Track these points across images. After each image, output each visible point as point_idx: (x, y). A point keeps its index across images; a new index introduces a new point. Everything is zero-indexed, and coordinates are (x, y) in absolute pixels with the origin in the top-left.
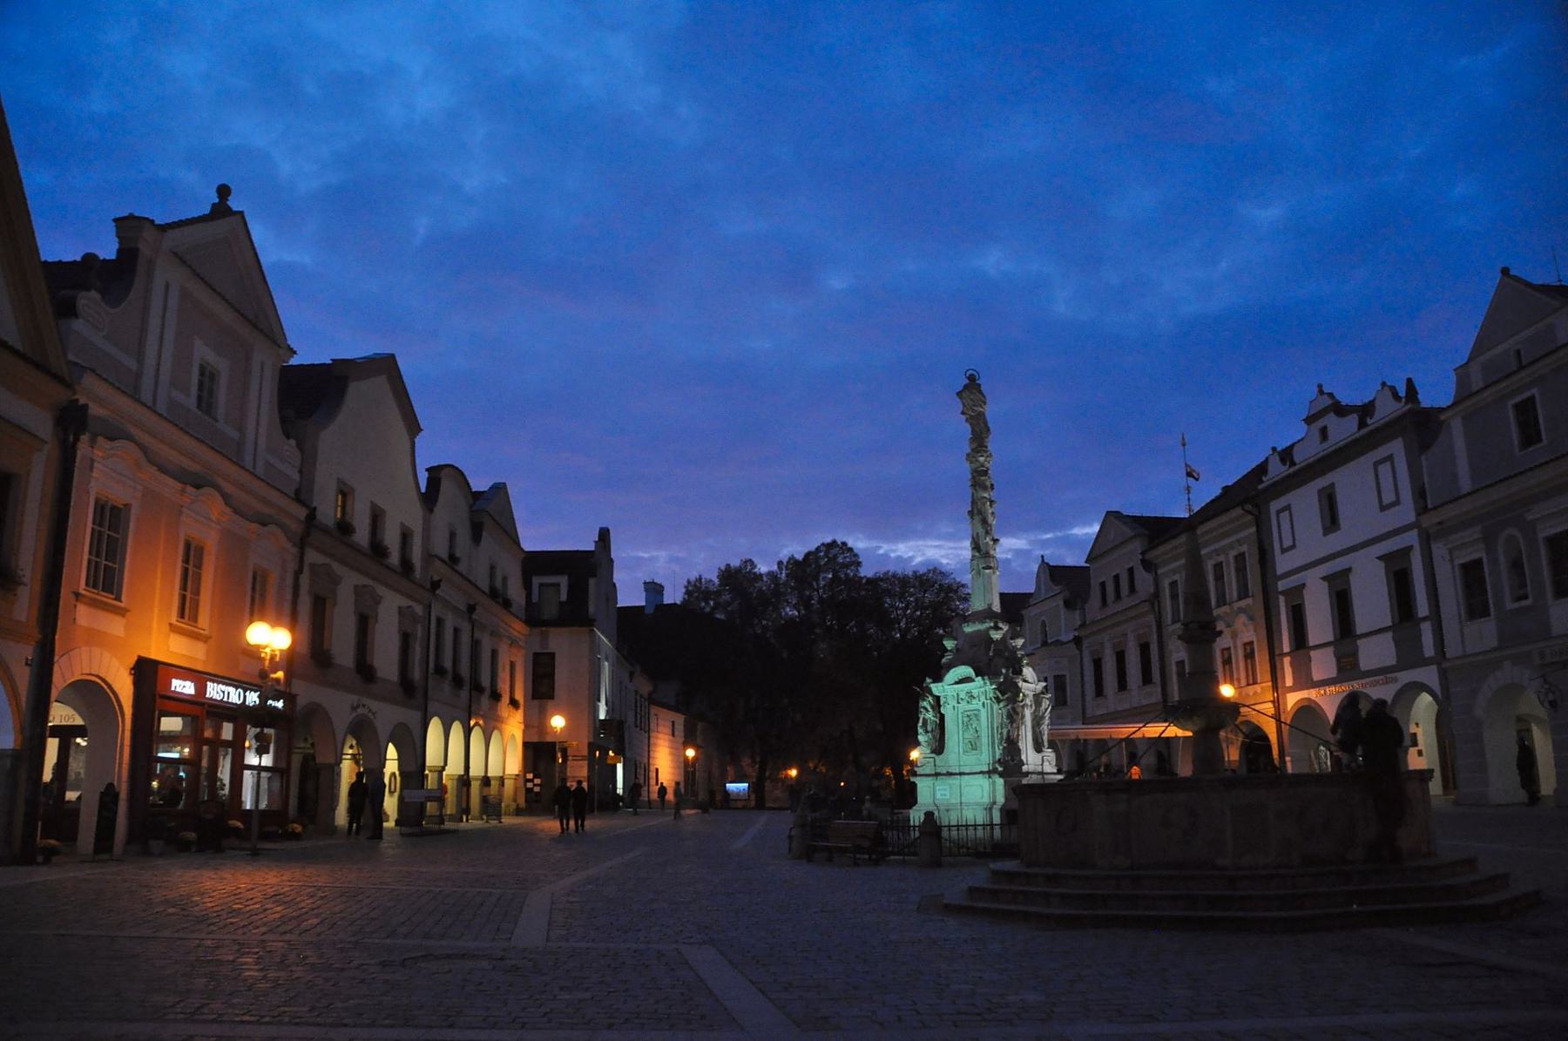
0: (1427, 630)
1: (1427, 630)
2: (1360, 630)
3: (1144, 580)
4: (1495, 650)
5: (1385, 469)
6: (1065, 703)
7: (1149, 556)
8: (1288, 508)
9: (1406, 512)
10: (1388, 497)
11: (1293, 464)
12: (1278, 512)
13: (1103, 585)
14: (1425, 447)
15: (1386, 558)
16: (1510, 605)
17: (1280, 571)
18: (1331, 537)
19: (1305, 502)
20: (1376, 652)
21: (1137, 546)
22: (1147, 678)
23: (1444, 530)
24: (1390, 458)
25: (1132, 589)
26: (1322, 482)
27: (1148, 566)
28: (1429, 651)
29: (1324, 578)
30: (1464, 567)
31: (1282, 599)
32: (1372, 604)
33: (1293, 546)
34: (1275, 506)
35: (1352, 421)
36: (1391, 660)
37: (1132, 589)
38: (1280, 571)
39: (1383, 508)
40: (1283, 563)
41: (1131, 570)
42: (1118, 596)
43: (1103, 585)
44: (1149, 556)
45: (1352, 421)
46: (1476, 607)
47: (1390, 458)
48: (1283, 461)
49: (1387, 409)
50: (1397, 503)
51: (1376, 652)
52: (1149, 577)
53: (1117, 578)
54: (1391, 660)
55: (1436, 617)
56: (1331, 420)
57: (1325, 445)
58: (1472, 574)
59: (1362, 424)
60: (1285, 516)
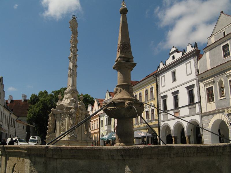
0: (197, 106)
2: (180, 106)
4: (215, 110)
5: (188, 65)
6: (110, 124)
9: (194, 76)
10: (189, 72)
11: (166, 65)
14: (198, 59)
15: (188, 88)
18: (175, 83)
19: (168, 75)
20: (184, 112)
26: (173, 70)
29: (171, 93)
30: (207, 89)
31: (161, 98)
32: (183, 99)
33: (165, 86)
35: (181, 53)
38: (161, 92)
40: (162, 90)
47: (190, 62)
48: (163, 64)
49: (189, 49)
50: (191, 74)
55: (200, 102)
58: (210, 92)
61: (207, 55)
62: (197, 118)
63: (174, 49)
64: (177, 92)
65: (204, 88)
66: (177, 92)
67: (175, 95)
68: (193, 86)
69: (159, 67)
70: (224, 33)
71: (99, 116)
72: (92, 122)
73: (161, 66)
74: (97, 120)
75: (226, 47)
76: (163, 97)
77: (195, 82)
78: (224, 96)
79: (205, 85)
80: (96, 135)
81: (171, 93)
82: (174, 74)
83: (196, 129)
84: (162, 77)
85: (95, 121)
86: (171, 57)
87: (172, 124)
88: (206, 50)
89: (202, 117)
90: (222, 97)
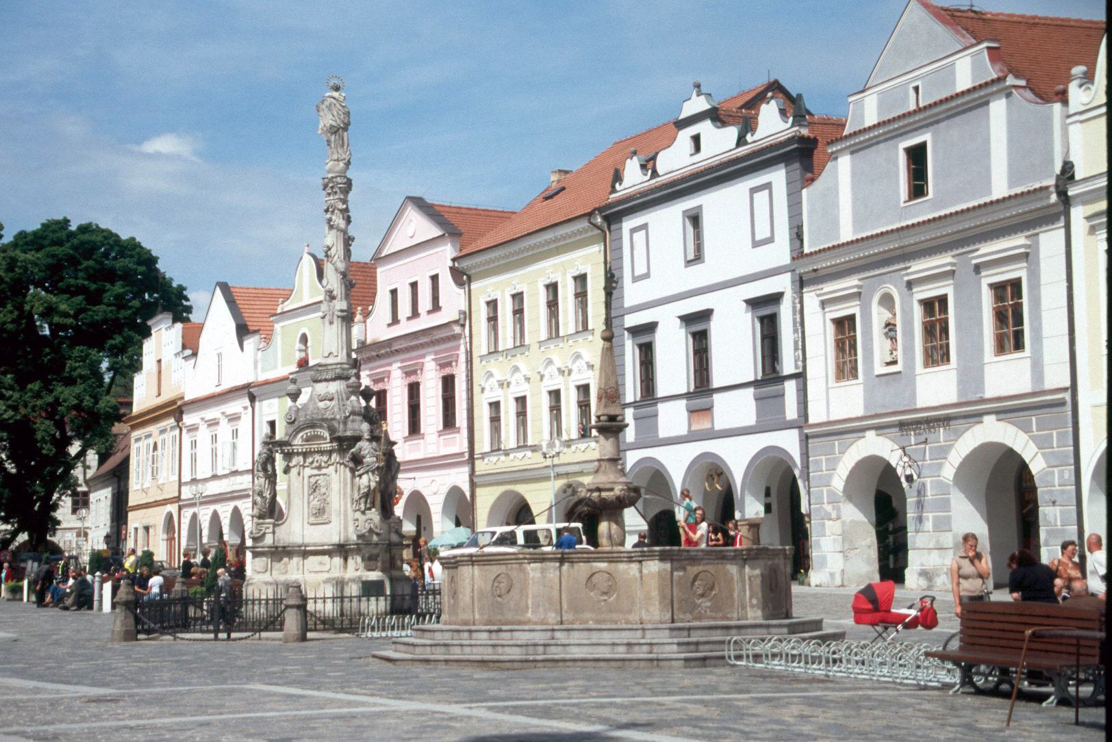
0: (790, 387)
1: (790, 387)
2: (716, 382)
3: (453, 299)
5: (761, 197)
7: (465, 264)
8: (644, 227)
9: (780, 253)
10: (762, 232)
11: (655, 174)
12: (633, 231)
13: (394, 292)
15: (754, 303)
16: (880, 369)
17: (628, 303)
19: (667, 221)
20: (736, 409)
21: (447, 252)
22: (449, 421)
23: (818, 278)
24: (768, 186)
25: (436, 307)
26: (689, 203)
27: (461, 276)
28: (791, 412)
29: (680, 317)
32: (735, 353)
33: (646, 276)
34: (628, 224)
35: (732, 132)
36: (750, 419)
37: (436, 307)
38: (628, 303)
39: (756, 244)
40: (632, 294)
41: (435, 279)
42: (415, 314)
43: (394, 292)
44: (465, 264)
45: (732, 132)
46: (846, 368)
47: (768, 186)
50: (770, 240)
51: (736, 409)
52: (461, 292)
53: (414, 286)
54: (750, 419)
55: (801, 377)
56: (705, 128)
57: (698, 157)
59: (741, 141)
60: (639, 237)
61: (842, 169)
62: (789, 441)
63: (698, 104)
64: (706, 315)
65: (820, 315)
66: (706, 315)
67: (698, 325)
68: (776, 298)
69: (618, 177)
70: (916, 89)
71: (252, 399)
72: (193, 429)
73: (634, 178)
74: (234, 418)
75: (917, 156)
76: (636, 331)
77: (783, 284)
78: (894, 362)
79: (823, 304)
80: (230, 506)
81: (680, 317)
82: (695, 219)
83: (784, 489)
84: (633, 231)
85: (213, 423)
86: (685, 135)
87: (677, 463)
88: (838, 151)
89: (805, 439)
90: (888, 364)
